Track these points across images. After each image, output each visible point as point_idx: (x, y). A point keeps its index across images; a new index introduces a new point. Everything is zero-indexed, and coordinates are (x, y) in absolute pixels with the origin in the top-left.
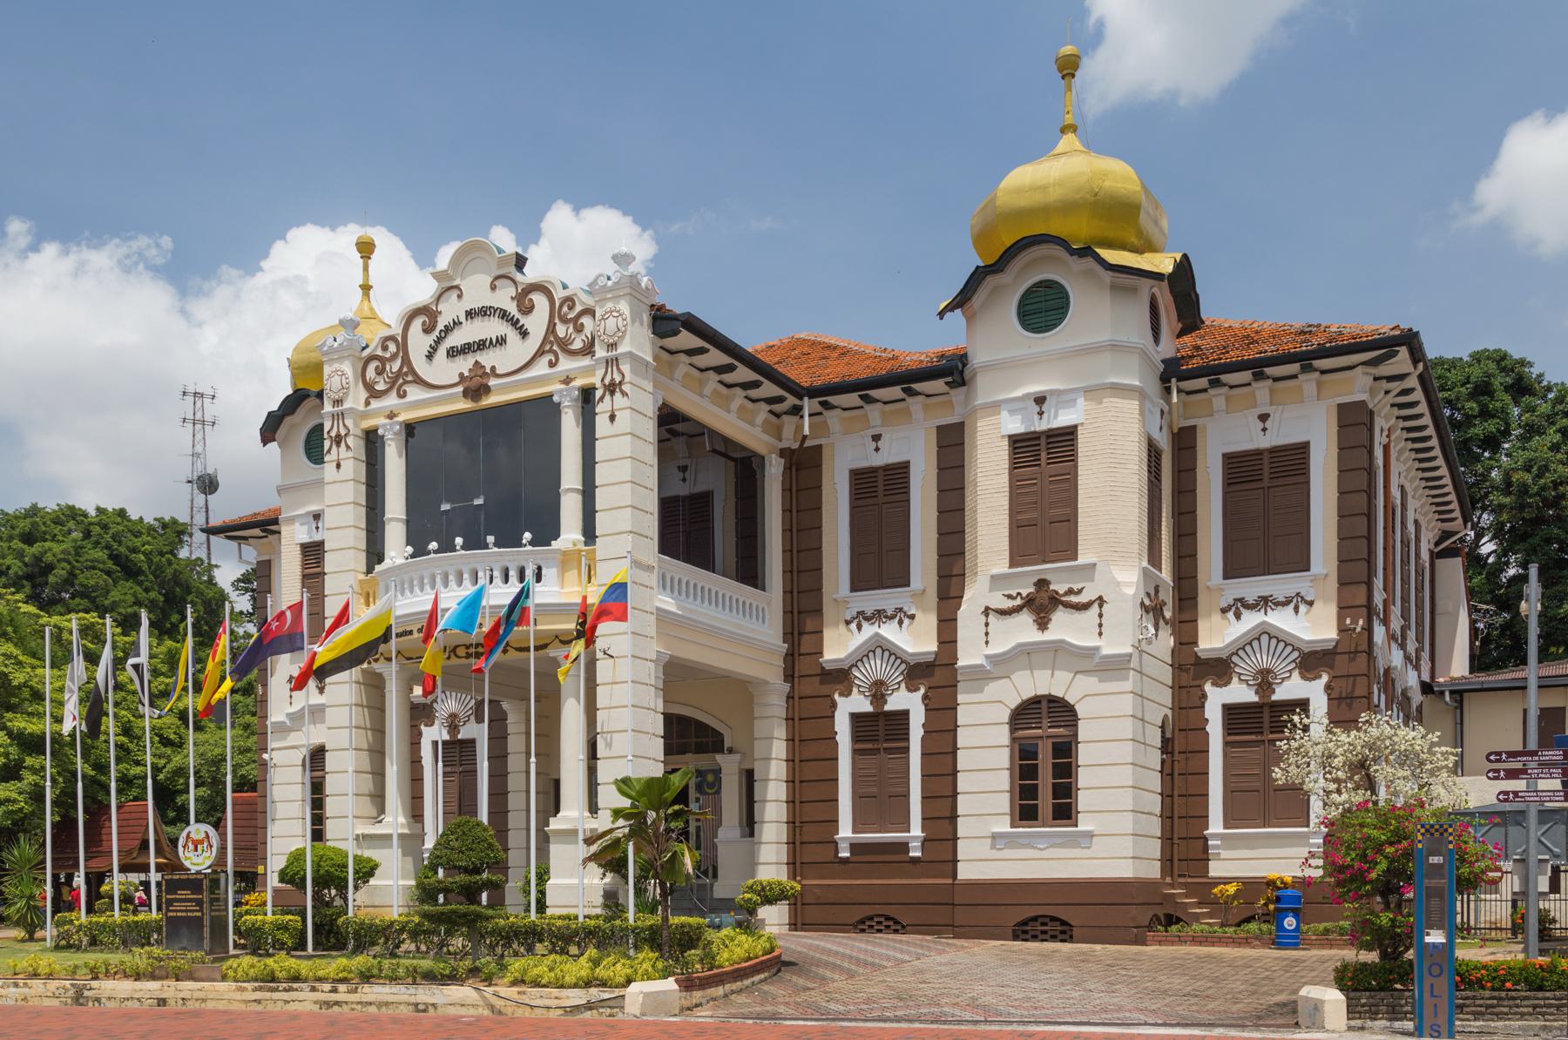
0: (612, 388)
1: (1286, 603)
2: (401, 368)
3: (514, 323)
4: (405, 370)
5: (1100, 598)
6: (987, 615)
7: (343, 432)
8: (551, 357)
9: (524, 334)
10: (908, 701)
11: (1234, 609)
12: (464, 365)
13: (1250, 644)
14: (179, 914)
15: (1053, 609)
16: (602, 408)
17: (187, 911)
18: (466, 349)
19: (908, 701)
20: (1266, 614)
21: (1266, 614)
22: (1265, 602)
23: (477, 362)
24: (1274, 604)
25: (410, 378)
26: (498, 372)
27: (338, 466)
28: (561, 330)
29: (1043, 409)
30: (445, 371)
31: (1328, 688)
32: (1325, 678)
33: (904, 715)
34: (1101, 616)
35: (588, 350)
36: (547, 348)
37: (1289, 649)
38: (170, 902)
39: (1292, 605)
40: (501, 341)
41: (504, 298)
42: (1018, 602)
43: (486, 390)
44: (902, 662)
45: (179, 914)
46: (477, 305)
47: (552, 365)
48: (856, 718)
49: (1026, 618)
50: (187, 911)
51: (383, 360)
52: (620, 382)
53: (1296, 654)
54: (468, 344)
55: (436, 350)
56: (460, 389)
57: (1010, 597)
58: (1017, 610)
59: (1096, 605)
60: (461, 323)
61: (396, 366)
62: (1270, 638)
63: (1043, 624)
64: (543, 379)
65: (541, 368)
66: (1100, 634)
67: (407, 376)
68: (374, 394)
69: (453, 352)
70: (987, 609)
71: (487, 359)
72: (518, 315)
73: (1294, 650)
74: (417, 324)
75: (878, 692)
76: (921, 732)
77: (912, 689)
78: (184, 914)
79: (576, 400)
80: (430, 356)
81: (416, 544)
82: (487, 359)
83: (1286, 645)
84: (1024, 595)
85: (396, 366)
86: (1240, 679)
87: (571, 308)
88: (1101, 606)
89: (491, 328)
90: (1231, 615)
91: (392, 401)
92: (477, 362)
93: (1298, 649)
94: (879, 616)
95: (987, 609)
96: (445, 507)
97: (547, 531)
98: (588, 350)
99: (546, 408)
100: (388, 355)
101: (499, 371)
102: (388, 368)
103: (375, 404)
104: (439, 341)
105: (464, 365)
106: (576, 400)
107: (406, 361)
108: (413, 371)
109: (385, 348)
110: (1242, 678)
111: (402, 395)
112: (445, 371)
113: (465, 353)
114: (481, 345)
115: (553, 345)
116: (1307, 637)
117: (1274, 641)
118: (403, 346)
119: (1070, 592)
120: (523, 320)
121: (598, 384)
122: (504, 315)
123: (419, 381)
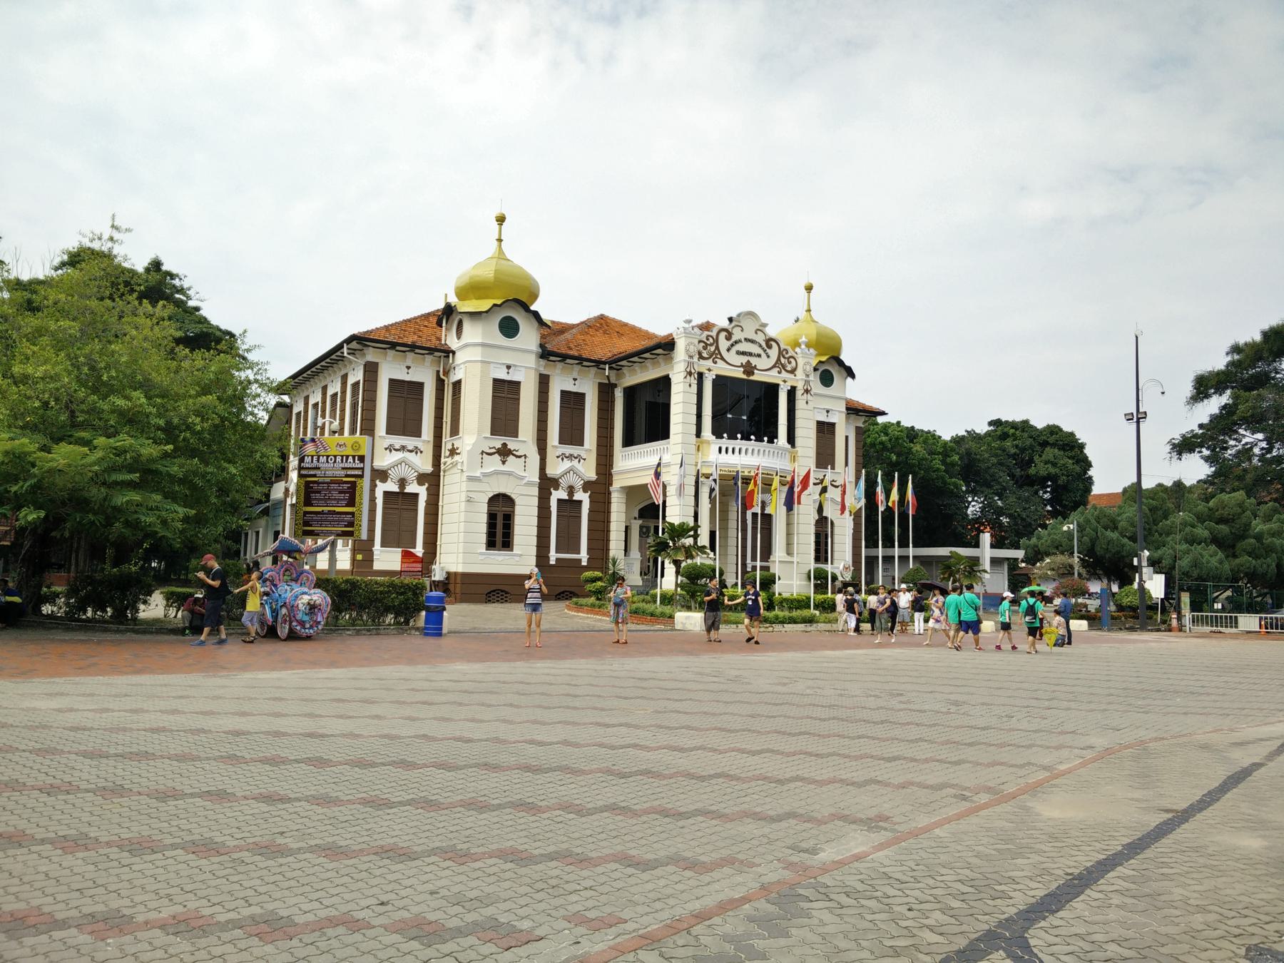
0: (807, 391)
3: (765, 351)
7: (693, 371)
9: (768, 357)
12: (744, 359)
18: (744, 353)
23: (748, 361)
27: (690, 386)
28: (783, 360)
35: (793, 371)
40: (759, 356)
41: (760, 338)
43: (753, 374)
46: (750, 337)
47: (779, 373)
56: (742, 369)
61: (713, 348)
64: (772, 377)
65: (774, 372)
67: (716, 355)
68: (701, 357)
71: (754, 361)
74: (723, 334)
80: (728, 350)
87: (787, 353)
91: (709, 363)
92: (748, 361)
96: (729, 416)
97: (773, 437)
98: (793, 371)
99: (773, 389)
100: (708, 342)
102: (709, 347)
103: (702, 362)
104: (732, 345)
105: (744, 359)
107: (717, 348)
109: (708, 339)
112: (732, 357)
114: (751, 354)
118: (716, 341)
120: (768, 351)
122: (760, 346)
123: (722, 359)
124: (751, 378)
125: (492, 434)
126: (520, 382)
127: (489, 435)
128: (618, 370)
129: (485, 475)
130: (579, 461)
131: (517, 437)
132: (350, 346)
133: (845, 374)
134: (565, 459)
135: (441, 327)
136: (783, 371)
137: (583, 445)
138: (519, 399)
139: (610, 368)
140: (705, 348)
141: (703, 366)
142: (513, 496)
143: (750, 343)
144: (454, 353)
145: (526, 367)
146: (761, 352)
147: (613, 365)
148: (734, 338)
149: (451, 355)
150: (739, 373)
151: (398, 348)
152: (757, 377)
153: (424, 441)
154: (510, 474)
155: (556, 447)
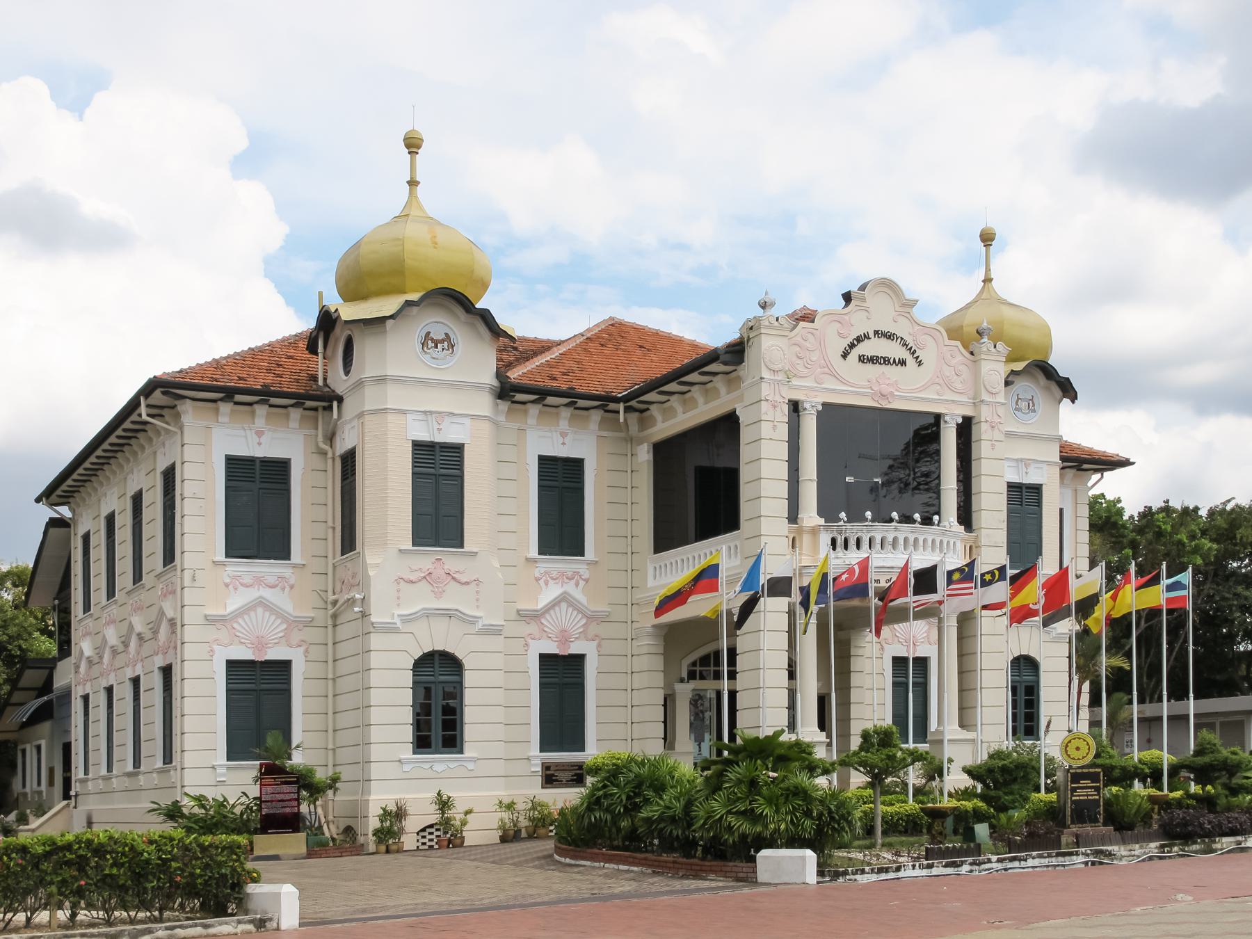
9: (920, 364)
14: (1081, 798)
17: (1087, 795)
18: (873, 360)
38: (1074, 790)
40: (903, 363)
45: (1081, 798)
50: (1087, 795)
55: (849, 353)
60: (869, 338)
69: (864, 359)
78: (1086, 798)
81: (827, 510)
104: (852, 346)
113: (873, 363)
114: (886, 361)
123: (834, 375)
125: (414, 545)
126: (463, 445)
127: (410, 547)
128: (642, 411)
129: (406, 619)
130: (577, 585)
131: (462, 546)
132: (151, 400)
133: (1058, 392)
134: (551, 582)
135: (317, 354)
137: (582, 554)
138: (461, 477)
139: (628, 409)
142: (459, 655)
143: (884, 341)
144: (340, 400)
145: (473, 417)
146: (903, 354)
147: (633, 403)
149: (335, 404)
151: (238, 398)
153: (295, 566)
154: (448, 614)
155: (534, 561)
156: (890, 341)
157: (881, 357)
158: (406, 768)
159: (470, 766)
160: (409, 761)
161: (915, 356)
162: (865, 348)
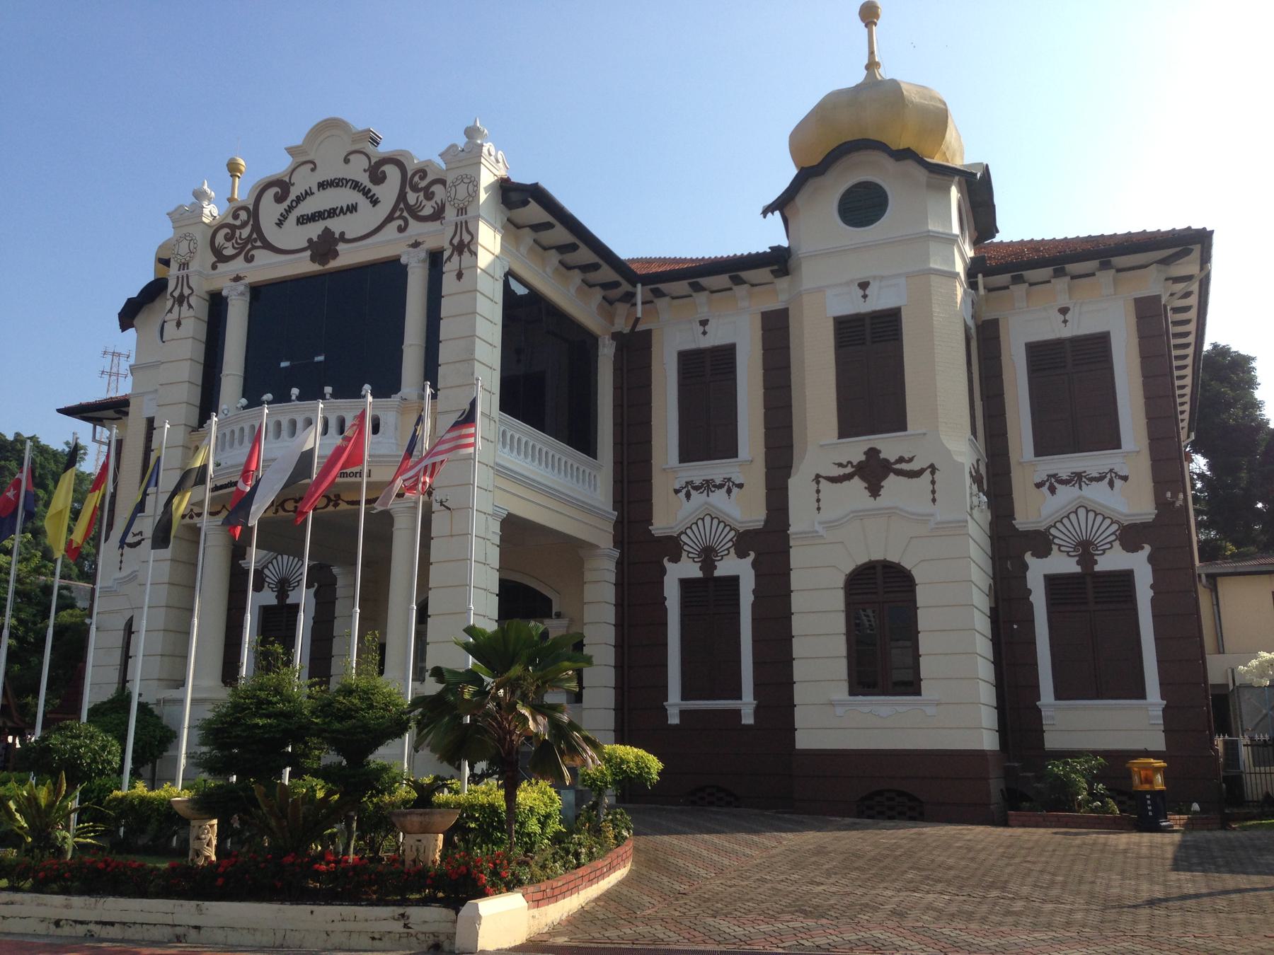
1: (1100, 479)
2: (250, 235)
3: (366, 193)
4: (255, 236)
5: (933, 469)
6: (818, 483)
8: (401, 222)
9: (375, 202)
10: (739, 568)
11: (1048, 484)
12: (314, 230)
13: (1068, 517)
15: (885, 477)
16: (450, 268)
19: (739, 568)
20: (1080, 488)
21: (1080, 488)
22: (1078, 478)
24: (1088, 479)
25: (259, 244)
26: (347, 236)
29: (867, 292)
30: (296, 236)
31: (1151, 559)
32: (1147, 549)
33: (734, 581)
34: (933, 482)
36: (398, 214)
37: (1108, 522)
39: (1107, 480)
40: (352, 208)
42: (849, 470)
43: (335, 254)
44: (731, 529)
47: (401, 229)
48: (685, 584)
49: (858, 484)
51: (233, 228)
52: (469, 243)
53: (1115, 527)
54: (319, 212)
57: (840, 465)
58: (848, 477)
59: (928, 473)
60: (312, 194)
61: (245, 232)
62: (1088, 511)
63: (875, 491)
66: (934, 500)
69: (303, 219)
70: (818, 476)
71: (336, 225)
72: (369, 185)
73: (1112, 523)
75: (708, 556)
76: (751, 598)
77: (741, 554)
79: (424, 261)
80: (280, 224)
82: (336, 225)
83: (1104, 518)
84: (855, 464)
85: (245, 232)
86: (1059, 549)
88: (933, 473)
89: (345, 196)
90: (1045, 489)
93: (1117, 522)
94: (708, 486)
95: (818, 476)
99: (393, 271)
101: (347, 236)
104: (290, 209)
106: (424, 261)
107: (257, 228)
108: (261, 236)
110: (1062, 548)
111: (249, 259)
113: (314, 221)
114: (332, 213)
115: (403, 211)
116: (1125, 510)
117: (1091, 515)
118: (254, 213)
119: (901, 460)
121: (447, 245)
123: (268, 246)
124: (334, 264)
136: (411, 221)
140: (228, 238)
141: (222, 279)
143: (331, 192)
146: (356, 197)
148: (294, 193)
150: (304, 265)
152: (347, 257)
156: (339, 188)
157: (325, 211)
158: (839, 711)
159: (930, 710)
160: (842, 704)
161: (369, 195)
162: (307, 208)
